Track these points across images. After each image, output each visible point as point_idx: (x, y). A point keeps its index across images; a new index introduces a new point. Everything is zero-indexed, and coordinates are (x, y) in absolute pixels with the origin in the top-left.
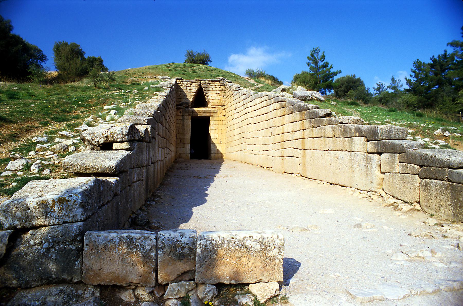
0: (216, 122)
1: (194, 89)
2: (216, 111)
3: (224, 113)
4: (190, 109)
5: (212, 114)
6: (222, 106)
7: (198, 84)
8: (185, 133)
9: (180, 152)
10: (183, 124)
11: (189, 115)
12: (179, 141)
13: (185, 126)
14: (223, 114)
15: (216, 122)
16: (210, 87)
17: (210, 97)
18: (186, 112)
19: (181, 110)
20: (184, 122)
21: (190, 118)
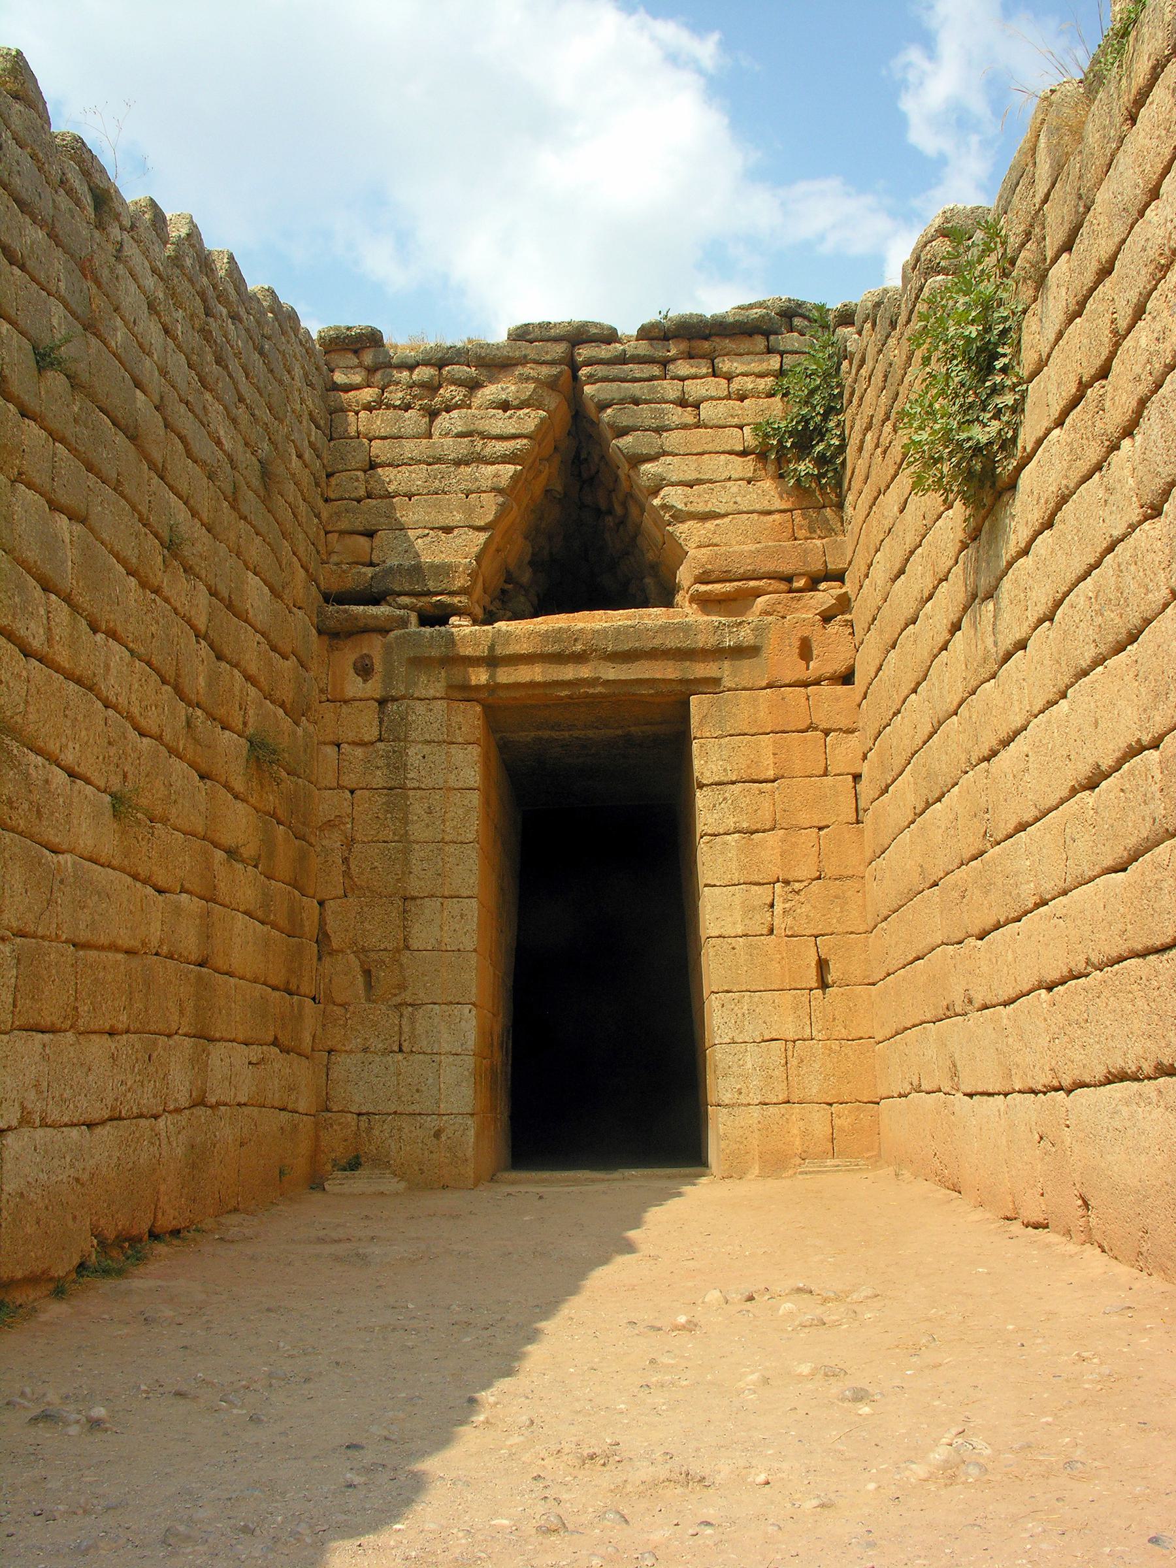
0: (765, 754)
1: (500, 423)
2: (745, 635)
3: (833, 650)
4: (461, 627)
5: (701, 670)
6: (814, 583)
7: (545, 371)
8: (415, 886)
9: (360, 1099)
10: (396, 791)
11: (462, 692)
12: (345, 975)
13: (417, 809)
14: (826, 662)
15: (765, 754)
16: (671, 389)
17: (674, 496)
18: (418, 662)
19: (374, 647)
20: (398, 765)
21: (470, 718)
